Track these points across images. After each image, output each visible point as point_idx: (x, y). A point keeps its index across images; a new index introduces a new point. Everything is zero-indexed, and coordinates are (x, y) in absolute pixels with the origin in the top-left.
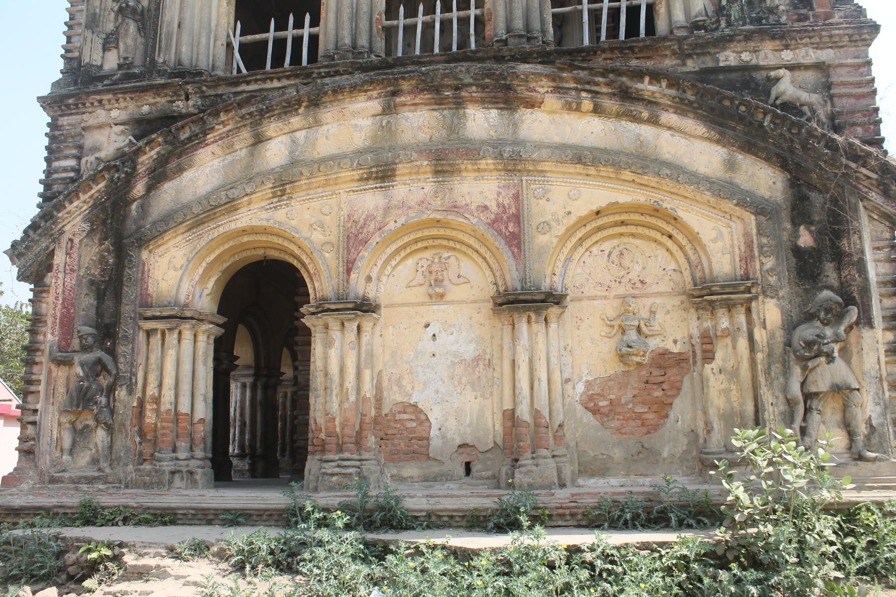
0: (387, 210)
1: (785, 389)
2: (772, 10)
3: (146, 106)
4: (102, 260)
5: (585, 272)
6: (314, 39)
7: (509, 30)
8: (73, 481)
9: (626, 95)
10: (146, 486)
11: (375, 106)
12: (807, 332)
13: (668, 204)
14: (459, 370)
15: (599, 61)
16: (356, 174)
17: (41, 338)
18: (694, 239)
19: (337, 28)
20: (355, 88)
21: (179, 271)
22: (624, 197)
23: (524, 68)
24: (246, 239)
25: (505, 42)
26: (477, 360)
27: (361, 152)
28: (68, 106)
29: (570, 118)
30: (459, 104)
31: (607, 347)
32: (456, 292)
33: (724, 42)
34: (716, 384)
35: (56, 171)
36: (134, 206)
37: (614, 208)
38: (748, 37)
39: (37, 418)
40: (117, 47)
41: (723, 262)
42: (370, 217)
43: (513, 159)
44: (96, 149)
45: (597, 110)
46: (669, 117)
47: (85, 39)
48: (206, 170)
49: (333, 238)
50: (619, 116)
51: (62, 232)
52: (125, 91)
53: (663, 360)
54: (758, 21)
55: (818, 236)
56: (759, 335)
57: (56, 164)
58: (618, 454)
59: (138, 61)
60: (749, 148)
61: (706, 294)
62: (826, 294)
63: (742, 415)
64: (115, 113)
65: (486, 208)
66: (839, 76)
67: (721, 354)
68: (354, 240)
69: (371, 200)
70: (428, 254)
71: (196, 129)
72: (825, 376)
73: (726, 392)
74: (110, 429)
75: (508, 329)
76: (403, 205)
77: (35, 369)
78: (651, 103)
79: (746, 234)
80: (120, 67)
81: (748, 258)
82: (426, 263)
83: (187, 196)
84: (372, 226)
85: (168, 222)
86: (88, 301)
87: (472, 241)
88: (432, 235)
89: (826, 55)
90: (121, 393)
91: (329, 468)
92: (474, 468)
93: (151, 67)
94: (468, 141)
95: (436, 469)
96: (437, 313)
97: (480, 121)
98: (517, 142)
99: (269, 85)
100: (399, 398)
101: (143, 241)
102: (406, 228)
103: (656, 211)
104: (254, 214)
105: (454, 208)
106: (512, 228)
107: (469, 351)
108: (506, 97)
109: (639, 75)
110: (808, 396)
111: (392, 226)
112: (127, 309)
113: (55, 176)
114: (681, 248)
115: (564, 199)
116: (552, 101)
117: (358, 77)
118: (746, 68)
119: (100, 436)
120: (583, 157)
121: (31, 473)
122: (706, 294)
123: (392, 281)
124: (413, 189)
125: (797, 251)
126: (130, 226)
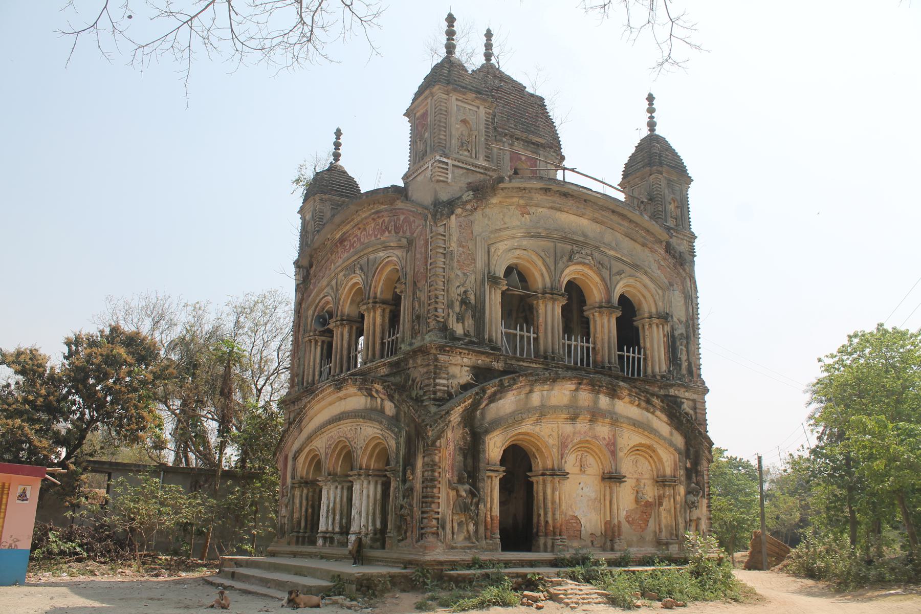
0: (574, 433)
1: (685, 518)
2: (684, 376)
3: (481, 361)
4: (464, 438)
5: (626, 467)
6: (536, 340)
7: (609, 363)
8: (461, 548)
9: (648, 402)
10: (491, 550)
11: (573, 387)
12: (691, 498)
13: (656, 446)
14: (590, 503)
15: (638, 384)
16: (566, 416)
17: (436, 474)
18: (660, 460)
19: (553, 344)
20: (570, 379)
21: (494, 447)
22: (643, 442)
23: (621, 384)
24: (521, 436)
25: (610, 368)
26: (596, 499)
27: (567, 407)
28: (445, 351)
29: (629, 406)
30: (598, 392)
31: (633, 497)
32: (589, 471)
33: (672, 386)
34: (664, 514)
35: (440, 385)
36: (478, 412)
37: (641, 445)
38: (679, 385)
39: (440, 516)
40: (463, 323)
41: (668, 471)
42: (568, 436)
43: (615, 420)
44: (454, 377)
45: (638, 406)
46: (658, 413)
47: (449, 315)
48: (508, 403)
49: (556, 443)
50: (643, 409)
51: (450, 421)
52: (474, 351)
53: (648, 504)
54: (680, 379)
55: (691, 463)
56: (678, 498)
57: (438, 381)
58: (635, 539)
59: (472, 334)
60: (677, 429)
61: (662, 481)
62: (693, 485)
63: (671, 526)
64: (465, 360)
65: (604, 439)
66: (698, 405)
67: (665, 503)
68: (563, 445)
69: (568, 428)
70: (580, 453)
71: (512, 382)
72: (696, 513)
73: (666, 518)
74: (476, 524)
75: (608, 488)
76: (579, 432)
77: (435, 490)
78: (654, 406)
79: (675, 461)
80: (465, 335)
81: (675, 470)
82: (579, 457)
83: (502, 413)
84: (570, 440)
85: (496, 424)
86: (460, 458)
87: (597, 451)
88: (585, 446)
89: (695, 396)
90: (481, 506)
91: (559, 542)
92: (595, 543)
93: (481, 342)
94: (600, 409)
95: (584, 543)
96: (583, 478)
97: (604, 401)
98: (615, 413)
99: (532, 365)
100: (571, 513)
101: (487, 432)
102: (580, 442)
103: (649, 447)
104: (526, 427)
105: (595, 437)
106: (612, 448)
107: (593, 495)
108: (613, 394)
109: (653, 395)
110: (691, 521)
111: (575, 441)
112: (482, 465)
113: (438, 387)
114: (655, 462)
115: (629, 438)
116: (627, 399)
117: (569, 373)
118: (676, 397)
119: (471, 527)
120: (636, 424)
121: (440, 544)
122: (662, 481)
123: (570, 464)
124: (582, 426)
125: (687, 469)
126: (477, 423)
